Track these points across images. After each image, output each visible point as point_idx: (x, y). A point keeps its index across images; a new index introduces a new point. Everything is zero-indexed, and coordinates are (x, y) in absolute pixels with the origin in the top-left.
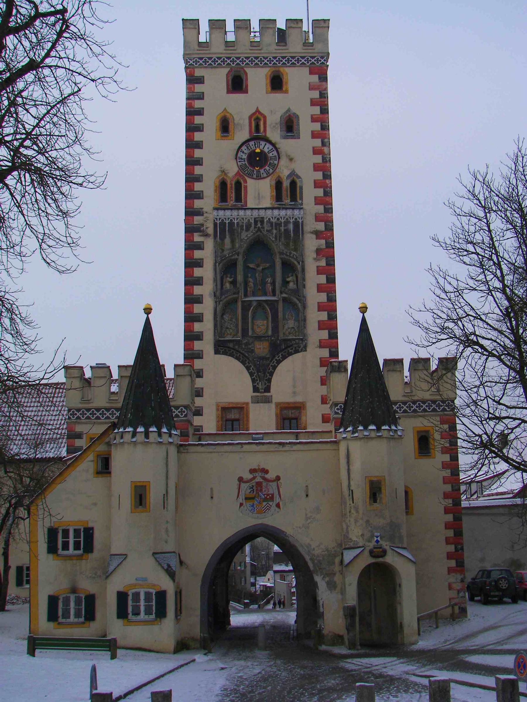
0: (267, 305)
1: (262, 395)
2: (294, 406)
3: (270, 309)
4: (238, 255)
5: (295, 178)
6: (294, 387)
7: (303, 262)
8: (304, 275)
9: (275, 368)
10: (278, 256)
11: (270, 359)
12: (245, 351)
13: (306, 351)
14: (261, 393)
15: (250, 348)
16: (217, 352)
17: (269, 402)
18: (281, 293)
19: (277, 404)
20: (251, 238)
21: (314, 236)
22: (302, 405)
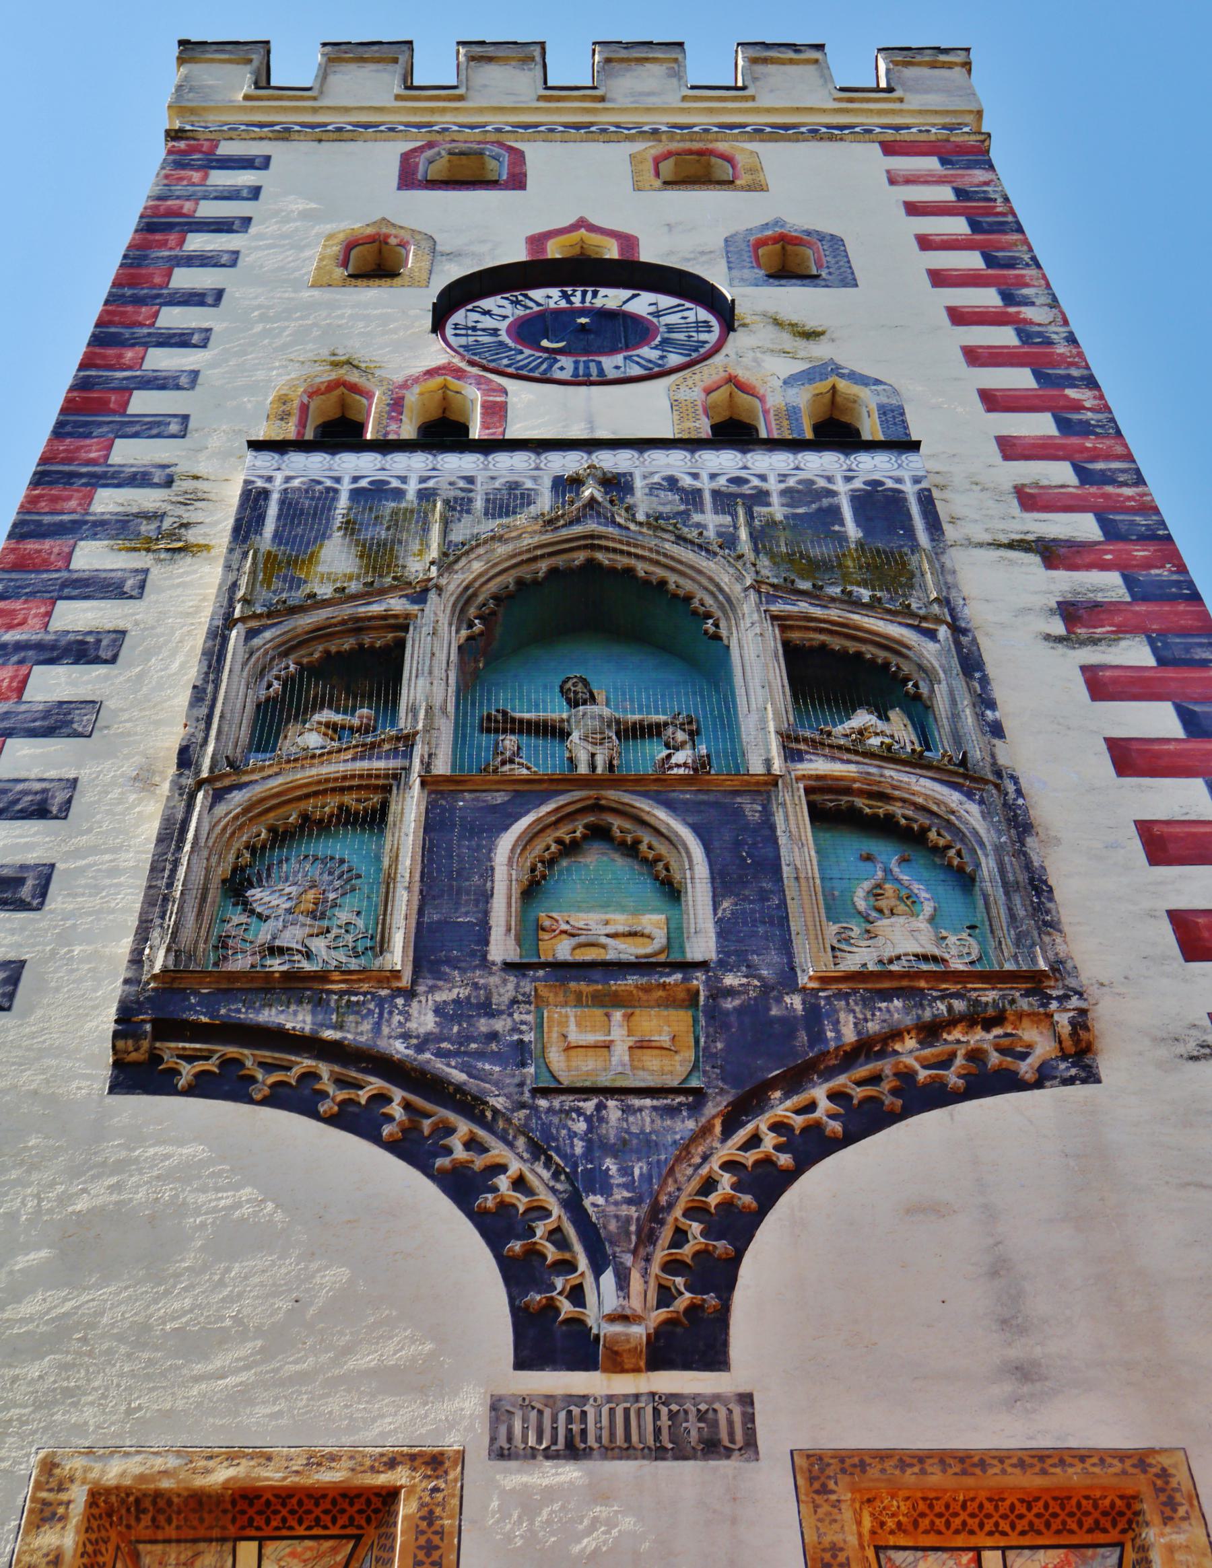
0: (670, 805)
1: (624, 1384)
2: (1032, 1481)
3: (696, 829)
4: (420, 597)
5: (843, 385)
6: (1011, 1322)
7: (957, 630)
8: (985, 681)
9: (768, 1184)
10: (749, 607)
11: (714, 1108)
12: (440, 1054)
13: (1090, 1076)
14: (616, 1363)
15: (493, 1036)
16: (136, 1074)
17: (712, 1448)
18: (792, 755)
19: (818, 1473)
20: (527, 541)
21: (1035, 559)
22: (1140, 1483)
